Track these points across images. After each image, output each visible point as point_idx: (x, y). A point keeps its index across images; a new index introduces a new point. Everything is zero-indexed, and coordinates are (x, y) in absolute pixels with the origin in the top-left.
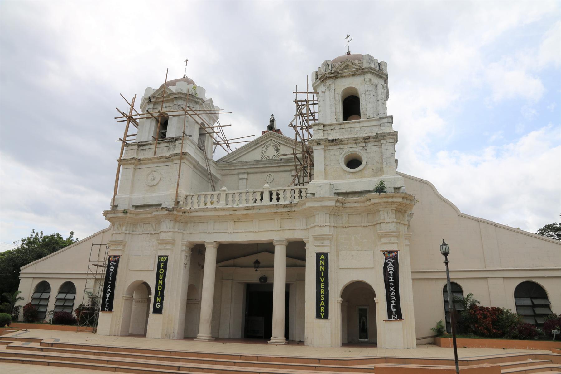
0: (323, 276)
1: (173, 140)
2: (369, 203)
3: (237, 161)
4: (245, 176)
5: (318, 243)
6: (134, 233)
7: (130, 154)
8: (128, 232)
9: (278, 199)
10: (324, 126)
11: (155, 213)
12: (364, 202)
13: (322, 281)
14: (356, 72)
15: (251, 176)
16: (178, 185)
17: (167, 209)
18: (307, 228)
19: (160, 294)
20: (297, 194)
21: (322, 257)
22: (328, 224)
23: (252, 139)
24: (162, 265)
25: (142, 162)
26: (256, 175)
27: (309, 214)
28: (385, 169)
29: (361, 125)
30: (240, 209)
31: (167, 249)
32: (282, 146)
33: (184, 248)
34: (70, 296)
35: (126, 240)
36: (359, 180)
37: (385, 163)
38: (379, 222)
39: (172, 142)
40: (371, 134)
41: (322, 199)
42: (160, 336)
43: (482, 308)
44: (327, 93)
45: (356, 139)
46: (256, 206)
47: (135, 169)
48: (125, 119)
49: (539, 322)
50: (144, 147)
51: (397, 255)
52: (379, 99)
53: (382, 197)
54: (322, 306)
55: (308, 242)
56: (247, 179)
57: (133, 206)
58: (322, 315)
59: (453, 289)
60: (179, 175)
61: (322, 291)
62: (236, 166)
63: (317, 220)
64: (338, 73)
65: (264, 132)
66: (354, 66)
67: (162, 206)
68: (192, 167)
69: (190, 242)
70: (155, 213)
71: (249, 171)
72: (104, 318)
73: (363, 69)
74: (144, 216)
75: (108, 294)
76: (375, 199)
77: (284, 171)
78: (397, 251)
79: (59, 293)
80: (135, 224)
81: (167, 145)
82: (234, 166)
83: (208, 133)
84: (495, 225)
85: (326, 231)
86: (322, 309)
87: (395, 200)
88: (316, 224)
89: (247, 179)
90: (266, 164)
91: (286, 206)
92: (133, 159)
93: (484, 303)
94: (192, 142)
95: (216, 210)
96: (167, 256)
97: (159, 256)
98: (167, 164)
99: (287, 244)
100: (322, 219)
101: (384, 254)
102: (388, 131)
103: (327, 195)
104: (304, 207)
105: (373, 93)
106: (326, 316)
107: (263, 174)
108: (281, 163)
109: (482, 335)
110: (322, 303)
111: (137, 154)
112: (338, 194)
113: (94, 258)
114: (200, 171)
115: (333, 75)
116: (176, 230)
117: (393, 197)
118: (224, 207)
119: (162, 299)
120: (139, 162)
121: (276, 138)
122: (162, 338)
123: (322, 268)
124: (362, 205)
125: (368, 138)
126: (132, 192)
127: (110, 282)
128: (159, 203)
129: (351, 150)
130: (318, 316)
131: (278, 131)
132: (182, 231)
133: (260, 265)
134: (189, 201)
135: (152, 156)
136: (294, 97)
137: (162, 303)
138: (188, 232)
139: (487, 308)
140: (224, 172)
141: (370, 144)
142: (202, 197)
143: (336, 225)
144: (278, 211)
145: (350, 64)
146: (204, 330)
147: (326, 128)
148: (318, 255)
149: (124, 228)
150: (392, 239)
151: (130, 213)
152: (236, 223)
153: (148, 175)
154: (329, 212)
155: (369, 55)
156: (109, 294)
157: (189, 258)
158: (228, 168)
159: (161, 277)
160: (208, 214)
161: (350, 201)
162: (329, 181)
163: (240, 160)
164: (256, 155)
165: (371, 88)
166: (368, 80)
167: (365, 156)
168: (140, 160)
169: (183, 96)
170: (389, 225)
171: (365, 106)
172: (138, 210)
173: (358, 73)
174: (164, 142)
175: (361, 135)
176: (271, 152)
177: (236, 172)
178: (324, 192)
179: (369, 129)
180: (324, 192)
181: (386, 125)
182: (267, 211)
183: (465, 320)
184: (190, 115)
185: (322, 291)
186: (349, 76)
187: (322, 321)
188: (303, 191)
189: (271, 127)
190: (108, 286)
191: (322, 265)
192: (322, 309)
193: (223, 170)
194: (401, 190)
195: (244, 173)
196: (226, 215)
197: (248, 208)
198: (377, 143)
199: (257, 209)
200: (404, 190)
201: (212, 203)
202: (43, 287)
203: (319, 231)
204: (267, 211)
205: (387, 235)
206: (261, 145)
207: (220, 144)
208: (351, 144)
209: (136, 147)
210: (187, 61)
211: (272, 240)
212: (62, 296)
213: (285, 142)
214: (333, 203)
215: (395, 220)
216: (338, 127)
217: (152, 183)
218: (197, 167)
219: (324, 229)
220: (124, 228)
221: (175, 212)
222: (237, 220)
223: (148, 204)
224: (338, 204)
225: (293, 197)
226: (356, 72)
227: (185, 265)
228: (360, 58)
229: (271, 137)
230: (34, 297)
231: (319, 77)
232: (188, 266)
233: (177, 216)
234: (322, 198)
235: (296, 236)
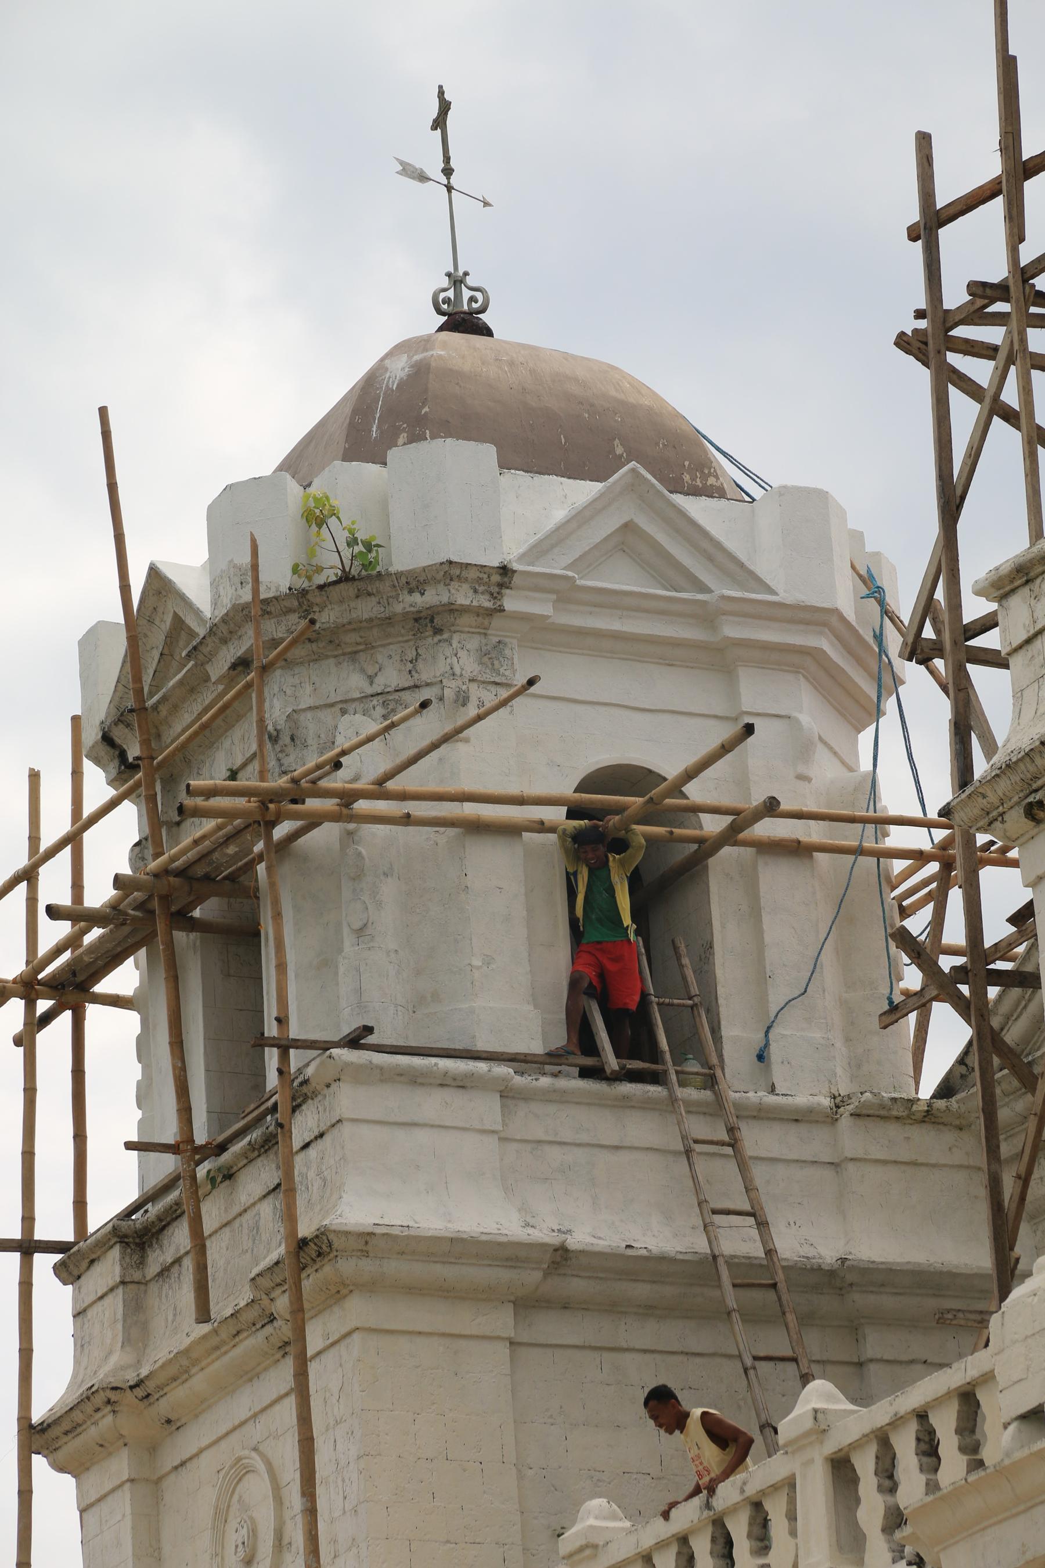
68: (501, 1321)
83: (707, 848)
94: (437, 1060)
114: (649, 1310)
184: (379, 790)
209: (109, 1268)
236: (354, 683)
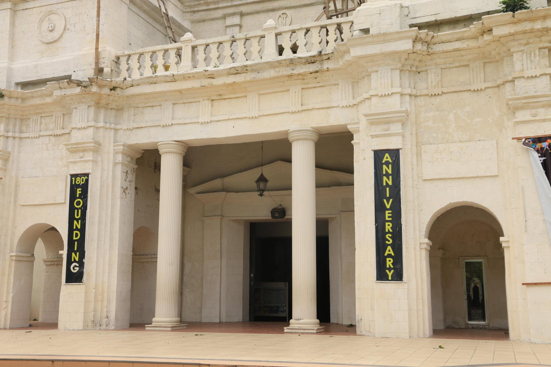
2: (487, 37)
4: (236, 20)
5: (378, 130)
6: (23, 135)
8: (10, 134)
11: (57, 93)
12: (475, 38)
13: (388, 206)
15: (247, 19)
16: (98, 36)
17: (79, 84)
18: (355, 102)
19: (77, 245)
20: (332, 36)
21: (387, 158)
22: (399, 90)
27: (358, 73)
30: (221, 74)
31: (86, 161)
33: (120, 158)
35: (10, 149)
38: (510, 78)
41: (385, 37)
42: (80, 325)
46: (251, 66)
47: (14, 11)
53: (520, 21)
54: (389, 256)
55: (358, 131)
56: (240, 26)
57: (17, 84)
58: (390, 274)
60: (98, 15)
61: (388, 227)
69: (130, 147)
70: (57, 93)
71: (244, 9)
74: (37, 101)
85: (394, 104)
88: (372, 93)
89: (240, 26)
91: (311, 61)
95: (174, 79)
96: (87, 175)
97: (72, 176)
99: (315, 137)
101: (524, 144)
103: (396, 28)
104: (347, 58)
106: (398, 276)
110: (389, 251)
114: (145, 11)
116: (101, 124)
118: (189, 72)
119: (82, 256)
122: (85, 328)
123: (387, 181)
124: (472, 44)
130: (381, 276)
133: (269, 184)
134: (123, 66)
137: (81, 264)
138: (125, 127)
140: (197, 16)
142: (147, 57)
143: (414, 92)
144: (295, 72)
146: (164, 310)
148: (378, 155)
150: (541, 111)
151: (10, 98)
152: (215, 103)
153: (41, 21)
154: (399, 65)
157: (131, 177)
158: (205, 8)
160: (159, 88)
161: (444, 39)
170: (533, 82)
172: (28, 92)
177: (220, 13)
178: (389, 23)
182: (272, 73)
185: (388, 227)
187: (390, 287)
188: (345, 28)
191: (387, 175)
192: (389, 262)
193: (194, 12)
195: (234, 14)
196: (193, 89)
197: (236, 72)
199: (253, 71)
201: (167, 68)
203: (377, 106)
204: (272, 73)
205: (529, 102)
211: (286, 133)
214: (407, 45)
217: (50, 37)
219: (389, 100)
221: (94, 89)
222: (217, 96)
224: (419, 46)
225: (324, 41)
227: (125, 190)
232: (131, 191)
234: (385, 34)
235: (333, 120)
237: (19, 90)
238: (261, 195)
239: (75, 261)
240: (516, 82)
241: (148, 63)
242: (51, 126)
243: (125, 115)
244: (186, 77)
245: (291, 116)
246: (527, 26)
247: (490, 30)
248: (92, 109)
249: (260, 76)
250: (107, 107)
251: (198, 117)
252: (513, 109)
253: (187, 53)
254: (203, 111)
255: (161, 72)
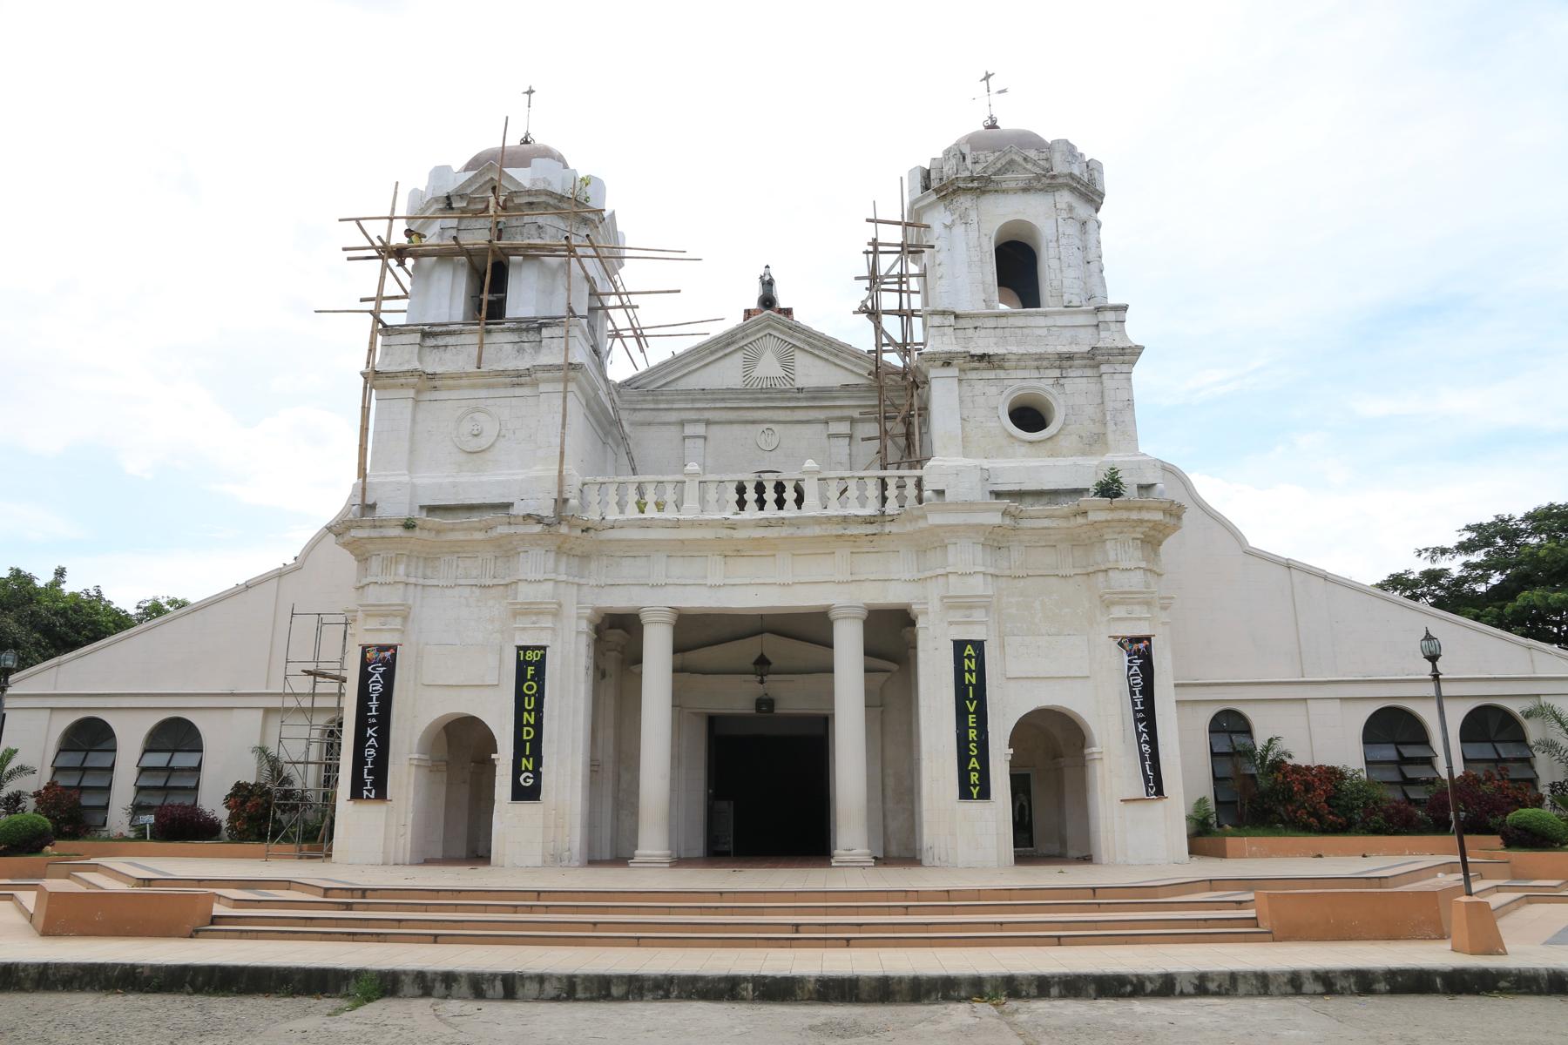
0: (971, 697)
1: (534, 327)
2: (1080, 520)
3: (673, 387)
4: (700, 429)
5: (957, 616)
7: (405, 357)
8: (412, 580)
9: (799, 501)
10: (957, 316)
12: (1066, 517)
14: (1035, 184)
15: (714, 429)
16: (562, 453)
17: (540, 520)
18: (921, 576)
19: (529, 747)
21: (969, 650)
22: (982, 569)
23: (717, 330)
24: (530, 671)
25: (437, 383)
26: (728, 427)
27: (930, 544)
28: (1110, 437)
29: (1049, 321)
31: (542, 629)
32: (798, 354)
33: (584, 626)
34: (183, 760)
36: (1050, 461)
37: (1111, 427)
39: (527, 330)
40: (1074, 349)
41: (968, 506)
42: (538, 861)
43: (1296, 769)
44: (959, 229)
45: (1040, 357)
47: (416, 401)
48: (373, 253)
49: (1412, 796)
50: (441, 341)
51: (1148, 648)
52: (1090, 258)
53: (1116, 508)
54: (974, 769)
56: (705, 438)
57: (422, 507)
58: (975, 792)
59: (1229, 725)
60: (564, 427)
62: (673, 401)
63: (951, 559)
64: (989, 180)
65: (748, 313)
66: (1029, 166)
67: (513, 511)
69: (596, 610)
70: (502, 530)
72: (352, 819)
73: (1054, 177)
74: (459, 536)
75: (370, 753)
76: (1101, 512)
77: (808, 422)
78: (1148, 639)
79: (146, 751)
80: (429, 558)
81: (514, 337)
82: (668, 402)
84: (1326, 577)
85: (978, 586)
86: (974, 777)
87: (1146, 515)
88: (949, 569)
89: (705, 438)
90: (757, 400)
91: (869, 520)
92: (412, 373)
93: (1301, 758)
95: (677, 524)
96: (544, 648)
97: (519, 648)
98: (518, 391)
99: (864, 615)
100: (965, 557)
101: (1120, 644)
102: (1121, 345)
104: (921, 524)
105: (1077, 242)
107: (749, 427)
108: (798, 399)
109: (1307, 829)
110: (974, 763)
111: (420, 360)
112: (998, 495)
113: (303, 653)
115: (975, 184)
116: (564, 577)
117: (1140, 509)
119: (538, 762)
120: (429, 381)
121: (781, 332)
123: (970, 678)
124: (1063, 524)
125: (1070, 357)
126: (411, 467)
127: (375, 716)
128: (505, 501)
129: (1025, 384)
130: (965, 794)
131: (788, 312)
132: (577, 580)
135: (472, 368)
136: (869, 232)
139: (1308, 768)
140: (639, 416)
141: (1071, 373)
145: (1019, 159)
146: (653, 839)
147: (963, 323)
148: (959, 646)
149: (402, 569)
150: (1137, 608)
153: (460, 420)
155: (1067, 141)
156: (373, 752)
159: (529, 704)
160: (653, 534)
162: (977, 462)
163: (683, 385)
164: (728, 374)
165: (1071, 229)
166: (1064, 206)
167: (1061, 401)
168: (433, 376)
169: (552, 201)
170: (1126, 574)
171: (1053, 272)
172: (436, 520)
173: (1039, 186)
174: (503, 331)
175: (1050, 349)
176: (769, 367)
177: (674, 416)
178: (965, 488)
179: (1068, 333)
180: (965, 488)
181: (1112, 326)
183: (1257, 795)
185: (972, 734)
186: (1015, 191)
187: (974, 807)
189: (768, 301)
190: (370, 732)
192: (974, 777)
194: (1155, 493)
196: (704, 540)
198: (1089, 372)
199: (791, 525)
200: (1162, 492)
201: (660, 506)
202: (89, 736)
203: (957, 587)
204: (817, 531)
205: (1125, 598)
206: (742, 348)
207: (621, 337)
208: (1025, 368)
209: (417, 338)
210: (530, 92)
212: (160, 759)
213: (809, 344)
214: (996, 519)
215: (1143, 565)
216: (991, 323)
217: (473, 444)
218: (592, 403)
220: (402, 569)
221: (564, 529)
223: (468, 502)
224: (1008, 521)
226: (1035, 184)
228: (1027, 140)
229: (769, 326)
230: (59, 764)
231: (935, 184)
232: (591, 672)
233: (566, 537)
234: (971, 503)
235: (892, 596)
236: (562, 225)
237: (424, 514)
238: (762, 682)
239: (527, 770)
240: (1111, 573)
241: (632, 497)
242: (475, 573)
243: (593, 565)
244: (693, 524)
245: (841, 588)
246: (1124, 515)
247: (1085, 513)
248: (552, 555)
249: (799, 533)
250: (570, 554)
251: (705, 577)
252: (1108, 604)
253: (691, 490)
254: (715, 570)
255: (651, 513)
